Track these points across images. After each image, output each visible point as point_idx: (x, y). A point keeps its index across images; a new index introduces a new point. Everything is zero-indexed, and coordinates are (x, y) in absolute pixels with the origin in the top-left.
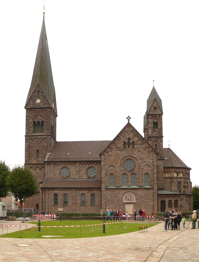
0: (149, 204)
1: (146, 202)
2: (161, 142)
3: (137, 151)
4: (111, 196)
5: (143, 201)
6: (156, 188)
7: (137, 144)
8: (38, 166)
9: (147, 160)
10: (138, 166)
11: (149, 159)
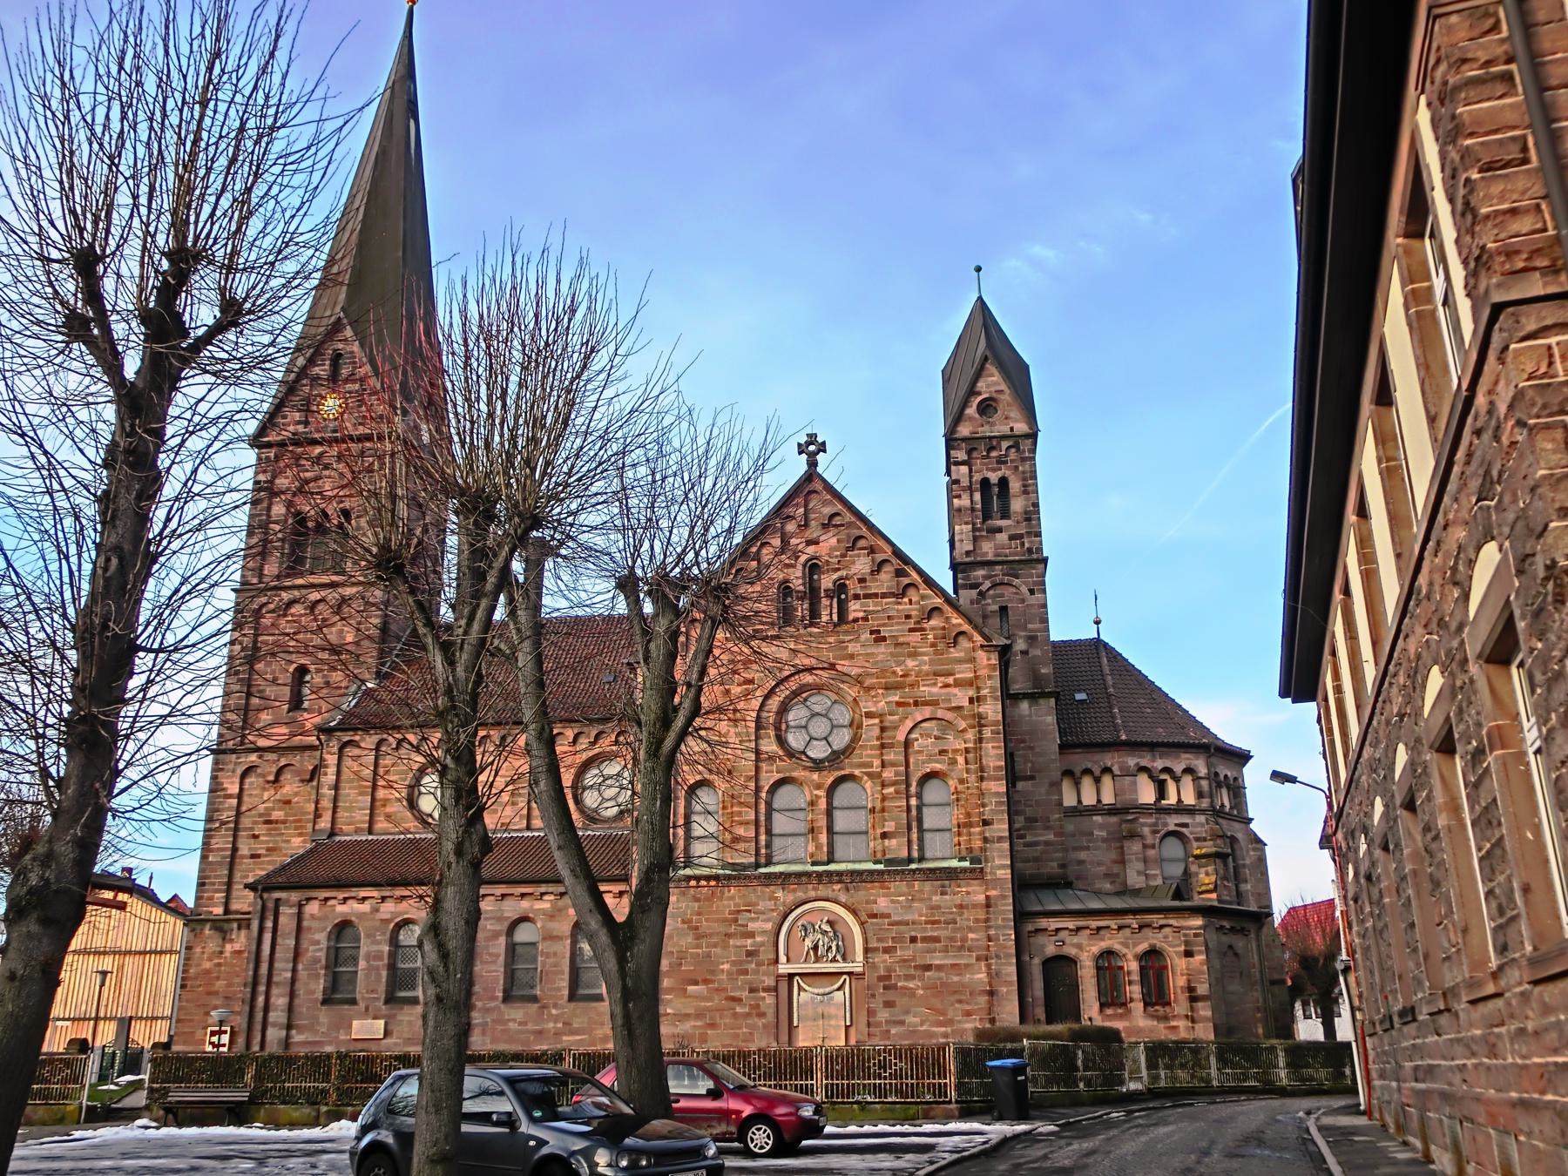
0: (956, 979)
1: (939, 968)
2: (1032, 592)
3: (866, 636)
4: (697, 928)
5: (914, 959)
6: (1003, 867)
7: (867, 596)
8: (296, 759)
9: (935, 690)
10: (877, 731)
11: (946, 686)
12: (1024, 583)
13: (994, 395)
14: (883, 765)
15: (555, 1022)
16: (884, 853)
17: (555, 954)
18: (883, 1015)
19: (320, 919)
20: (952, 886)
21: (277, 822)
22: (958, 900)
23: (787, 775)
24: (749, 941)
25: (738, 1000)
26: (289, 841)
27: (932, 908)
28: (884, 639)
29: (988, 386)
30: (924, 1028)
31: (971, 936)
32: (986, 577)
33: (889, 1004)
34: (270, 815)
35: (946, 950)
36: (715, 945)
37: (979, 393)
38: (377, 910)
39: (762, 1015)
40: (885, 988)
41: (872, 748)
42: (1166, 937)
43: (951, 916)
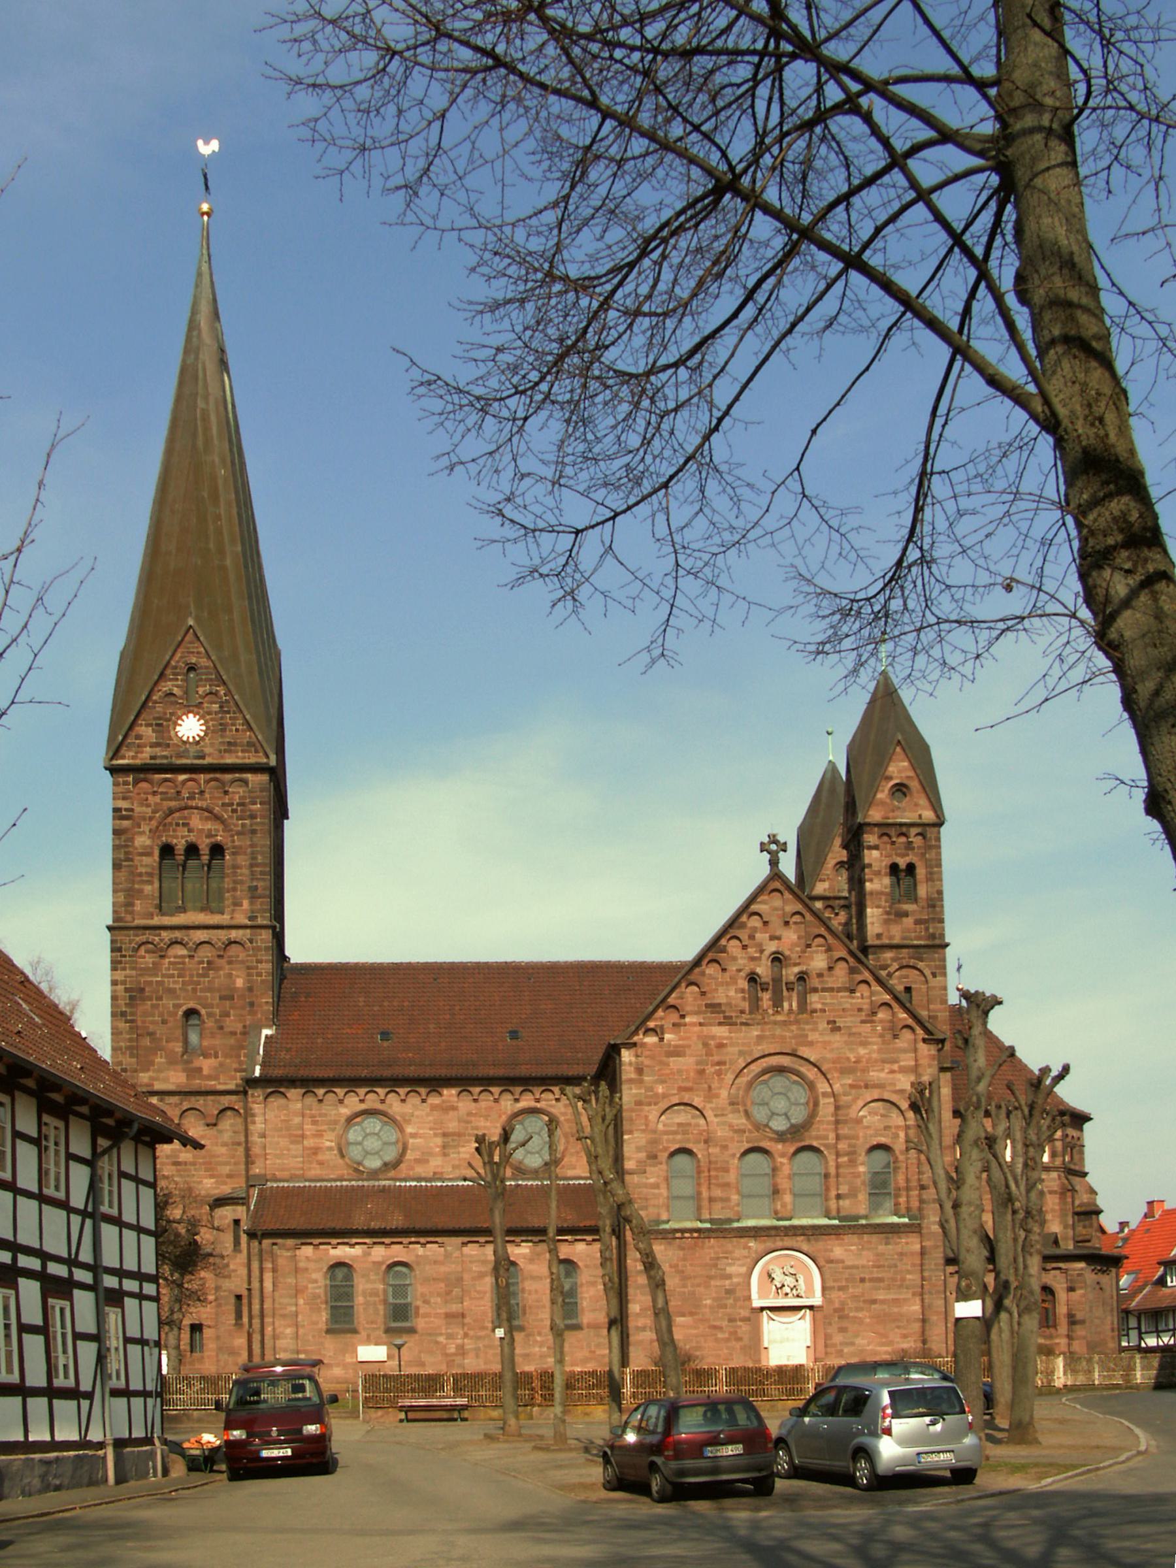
0: (896, 1310)
1: (883, 1302)
2: (934, 975)
3: (823, 1025)
4: (683, 1272)
5: (863, 1294)
6: (934, 1223)
7: (824, 990)
8: (200, 1102)
9: (882, 1075)
10: (832, 1109)
11: (892, 1072)
12: (928, 966)
13: (905, 782)
14: (838, 1138)
15: (540, 1347)
16: (838, 1211)
17: (536, 1291)
18: (838, 1338)
19: (316, 1261)
20: (894, 1238)
21: (186, 1163)
22: (899, 1248)
23: (756, 1145)
24: (727, 1282)
25: (720, 1328)
26: (201, 1182)
27: (877, 1255)
28: (839, 1029)
29: (900, 772)
30: (870, 1347)
31: (908, 1277)
32: (894, 960)
33: (842, 1330)
34: (178, 1157)
35: (888, 1288)
36: (699, 1285)
37: (890, 778)
38: (369, 1254)
39: (739, 1339)
40: (839, 1318)
41: (828, 1123)
42: (1055, 1276)
43: (892, 1262)
